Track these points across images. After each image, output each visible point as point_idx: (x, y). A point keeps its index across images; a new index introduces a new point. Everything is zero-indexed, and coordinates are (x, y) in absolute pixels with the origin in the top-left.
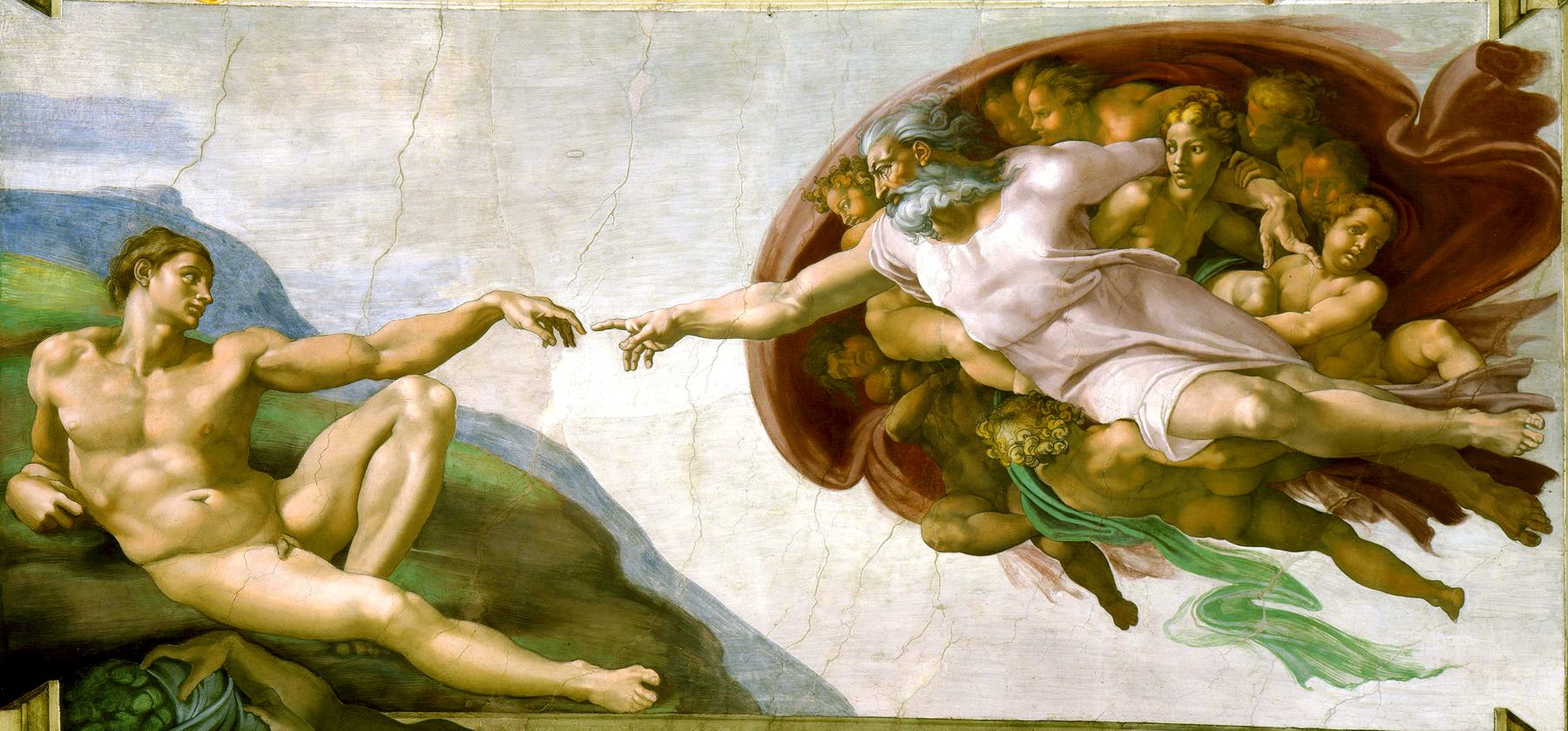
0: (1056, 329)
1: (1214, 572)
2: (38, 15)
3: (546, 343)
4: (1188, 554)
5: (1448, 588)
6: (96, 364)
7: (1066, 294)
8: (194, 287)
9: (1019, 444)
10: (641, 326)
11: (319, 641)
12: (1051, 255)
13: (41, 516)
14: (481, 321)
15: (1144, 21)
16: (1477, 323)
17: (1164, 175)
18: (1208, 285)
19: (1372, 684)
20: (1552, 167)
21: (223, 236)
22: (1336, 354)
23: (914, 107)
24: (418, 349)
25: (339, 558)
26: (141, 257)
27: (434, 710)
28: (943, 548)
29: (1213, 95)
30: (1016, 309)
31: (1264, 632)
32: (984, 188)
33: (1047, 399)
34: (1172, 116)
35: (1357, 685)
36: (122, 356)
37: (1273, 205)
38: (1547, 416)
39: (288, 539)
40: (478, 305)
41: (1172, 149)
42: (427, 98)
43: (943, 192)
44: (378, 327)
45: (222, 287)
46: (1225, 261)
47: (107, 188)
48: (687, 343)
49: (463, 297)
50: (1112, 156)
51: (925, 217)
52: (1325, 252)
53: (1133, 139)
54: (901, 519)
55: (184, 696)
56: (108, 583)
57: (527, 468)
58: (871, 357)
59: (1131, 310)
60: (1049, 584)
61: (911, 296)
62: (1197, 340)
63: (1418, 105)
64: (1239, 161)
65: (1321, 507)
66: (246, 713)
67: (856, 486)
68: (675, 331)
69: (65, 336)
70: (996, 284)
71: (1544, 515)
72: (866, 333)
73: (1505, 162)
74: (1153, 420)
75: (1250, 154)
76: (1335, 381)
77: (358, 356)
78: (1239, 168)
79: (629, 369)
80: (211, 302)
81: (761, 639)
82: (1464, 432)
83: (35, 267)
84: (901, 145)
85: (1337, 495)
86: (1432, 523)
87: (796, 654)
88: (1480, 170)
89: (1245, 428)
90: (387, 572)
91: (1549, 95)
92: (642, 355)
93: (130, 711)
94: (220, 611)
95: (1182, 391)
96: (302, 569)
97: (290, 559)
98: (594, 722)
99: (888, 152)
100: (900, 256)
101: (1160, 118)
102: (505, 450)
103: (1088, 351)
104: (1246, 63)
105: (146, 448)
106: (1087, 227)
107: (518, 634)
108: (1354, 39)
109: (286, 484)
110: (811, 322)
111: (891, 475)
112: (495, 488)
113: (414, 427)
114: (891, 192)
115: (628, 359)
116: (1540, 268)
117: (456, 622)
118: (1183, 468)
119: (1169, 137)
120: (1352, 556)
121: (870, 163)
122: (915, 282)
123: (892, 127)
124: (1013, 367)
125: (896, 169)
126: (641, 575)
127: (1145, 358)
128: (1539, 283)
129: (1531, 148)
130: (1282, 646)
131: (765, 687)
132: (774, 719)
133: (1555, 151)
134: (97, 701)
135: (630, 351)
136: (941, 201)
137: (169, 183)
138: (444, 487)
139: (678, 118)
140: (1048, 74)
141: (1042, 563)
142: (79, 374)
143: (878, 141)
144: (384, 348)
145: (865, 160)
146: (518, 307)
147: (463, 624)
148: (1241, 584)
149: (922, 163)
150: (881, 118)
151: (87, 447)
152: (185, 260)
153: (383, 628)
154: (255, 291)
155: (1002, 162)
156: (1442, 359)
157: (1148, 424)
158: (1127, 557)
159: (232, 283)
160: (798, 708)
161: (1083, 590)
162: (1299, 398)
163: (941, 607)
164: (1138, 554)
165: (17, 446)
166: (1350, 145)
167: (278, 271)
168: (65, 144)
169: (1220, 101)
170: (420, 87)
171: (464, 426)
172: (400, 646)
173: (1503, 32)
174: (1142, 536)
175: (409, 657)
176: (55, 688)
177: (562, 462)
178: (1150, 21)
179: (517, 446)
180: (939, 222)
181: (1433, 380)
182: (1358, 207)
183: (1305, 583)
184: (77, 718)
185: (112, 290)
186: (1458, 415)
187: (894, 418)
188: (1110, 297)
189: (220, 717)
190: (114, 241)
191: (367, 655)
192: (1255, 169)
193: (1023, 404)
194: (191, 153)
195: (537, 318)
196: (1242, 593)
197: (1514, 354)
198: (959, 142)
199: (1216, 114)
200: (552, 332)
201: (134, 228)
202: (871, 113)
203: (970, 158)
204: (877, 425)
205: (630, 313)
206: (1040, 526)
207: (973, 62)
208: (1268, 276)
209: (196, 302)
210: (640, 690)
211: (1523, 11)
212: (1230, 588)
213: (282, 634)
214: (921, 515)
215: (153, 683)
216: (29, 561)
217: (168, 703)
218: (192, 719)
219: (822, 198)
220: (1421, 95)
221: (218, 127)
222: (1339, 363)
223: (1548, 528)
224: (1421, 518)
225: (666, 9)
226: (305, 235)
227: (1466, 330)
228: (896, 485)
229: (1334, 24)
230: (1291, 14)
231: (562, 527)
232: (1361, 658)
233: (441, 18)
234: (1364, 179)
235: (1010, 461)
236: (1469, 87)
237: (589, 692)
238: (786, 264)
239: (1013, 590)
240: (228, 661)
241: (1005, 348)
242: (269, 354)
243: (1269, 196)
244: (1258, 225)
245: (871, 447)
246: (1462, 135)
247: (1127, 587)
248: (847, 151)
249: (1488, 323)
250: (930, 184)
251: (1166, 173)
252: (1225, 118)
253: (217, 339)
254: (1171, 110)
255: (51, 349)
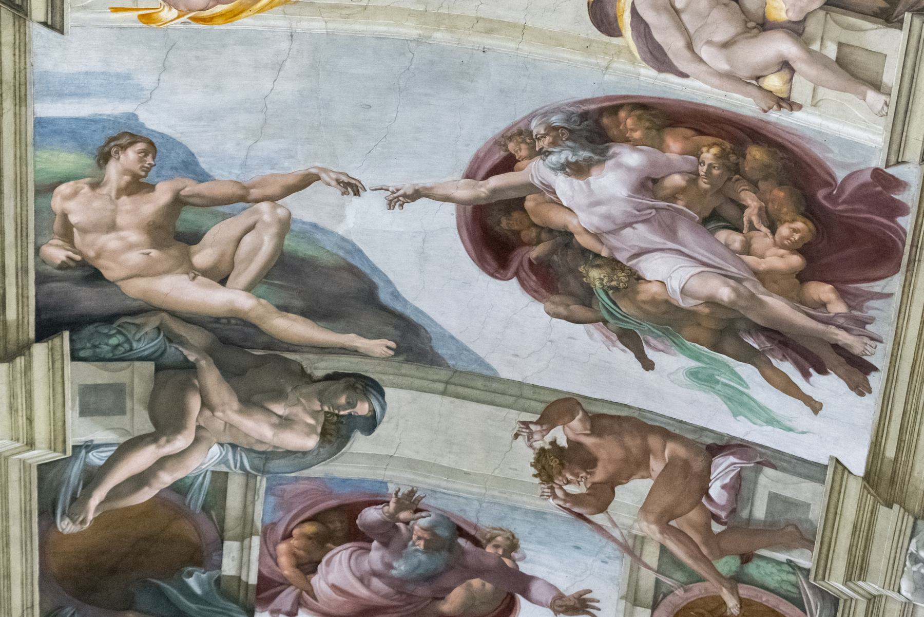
0: (628, 231)
1: (697, 359)
2: (58, 35)
3: (343, 194)
4: (684, 348)
5: (814, 400)
6: (89, 194)
7: (635, 216)
8: (145, 159)
9: (601, 279)
10: (398, 190)
11: (211, 317)
12: (629, 196)
13: (59, 262)
14: (307, 181)
15: (695, 101)
16: (849, 293)
17: (696, 175)
18: (712, 232)
19: (770, 428)
20: (901, 237)
21: (162, 135)
22: (775, 282)
23: (562, 112)
24: (269, 191)
25: (223, 282)
26: (115, 146)
27: (272, 350)
28: (555, 316)
29: (728, 145)
30: (608, 217)
31: (719, 390)
32: (596, 157)
33: (619, 262)
34: (704, 149)
35: (762, 426)
36: (104, 190)
37: (752, 205)
38: (878, 344)
39: (194, 272)
40: (306, 172)
41: (702, 164)
42: (281, 73)
43: (574, 155)
44: (248, 178)
45: (160, 159)
46: (724, 224)
47: (96, 114)
48: (423, 201)
49: (298, 167)
50: (668, 159)
51: (563, 164)
52: (776, 235)
53: (683, 153)
54: (534, 299)
55: (137, 337)
56: (96, 290)
57: (329, 249)
58: (527, 223)
59: (670, 232)
60: (609, 342)
61: (551, 198)
62: (703, 255)
63: (836, 185)
64: (737, 180)
65: (756, 346)
66: (170, 347)
67: (511, 280)
68: (416, 195)
69: (71, 183)
70: (598, 203)
71: (869, 385)
72: (524, 210)
73: (879, 227)
74: (675, 285)
75: (744, 178)
76: (774, 295)
77: (238, 191)
78: (737, 183)
79: (390, 209)
80: (155, 165)
81: (452, 337)
82: (835, 337)
83: (56, 153)
84: (550, 129)
85: (765, 344)
86: (811, 370)
87: (471, 347)
88: (862, 225)
89: (722, 300)
90: (249, 288)
91: (906, 203)
92: (398, 204)
93: (107, 344)
94: (157, 302)
95: (692, 276)
96: (201, 285)
97: (196, 281)
98: (360, 359)
99: (545, 130)
100: (546, 178)
101: (698, 148)
102: (318, 239)
103: (644, 245)
104: (748, 135)
105: (117, 231)
106: (651, 188)
107: (320, 321)
108: (807, 143)
109: (194, 248)
110: (493, 201)
111: (531, 279)
112: (311, 256)
113: (268, 225)
114: (544, 149)
115: (390, 204)
116: (886, 280)
117: (286, 313)
118: (685, 310)
119: (701, 158)
120: (769, 372)
121: (534, 134)
122: (554, 193)
123: (548, 119)
124: (602, 243)
125: (548, 139)
126: (389, 300)
127: (674, 256)
128: (885, 286)
129: (892, 224)
130: (728, 399)
131: (452, 357)
132: (456, 371)
133: (904, 230)
134: (89, 340)
135: (391, 201)
136: (572, 159)
137: (131, 111)
138: (282, 254)
139: (426, 95)
140: (638, 112)
141: (607, 334)
142: (80, 198)
143: (540, 124)
144: (253, 187)
145: (532, 132)
146: (329, 176)
147: (290, 315)
148: (710, 368)
149: (564, 139)
150: (542, 114)
151: (84, 231)
152: (140, 146)
153: (246, 313)
154: (180, 160)
155: (608, 148)
156: (829, 302)
157: (672, 288)
158: (653, 341)
159: (167, 156)
160: (469, 369)
161: (627, 349)
162: (753, 296)
163: (551, 341)
164: (658, 341)
165: (45, 232)
166: (798, 192)
167: (193, 150)
168: (72, 95)
169: (731, 149)
170: (279, 67)
171: (292, 227)
172: (256, 322)
173: (887, 166)
174: (661, 334)
175: (259, 327)
176: (66, 334)
177: (349, 247)
178: (698, 102)
179: (324, 238)
180: (570, 168)
181: (823, 310)
182: (798, 221)
183: (743, 376)
184: (78, 346)
185: (98, 161)
186: (832, 329)
187: (535, 253)
188: (659, 222)
189: (156, 347)
190: (99, 139)
191: (237, 324)
192: (745, 186)
193: (605, 261)
194: (144, 96)
195: (339, 182)
196: (710, 371)
197: (866, 313)
198: (585, 134)
199: (728, 154)
200: (347, 189)
201: (111, 133)
202: (538, 110)
203: (591, 142)
204: (525, 254)
205: (392, 185)
206: (607, 317)
207: (597, 98)
208: (745, 237)
209: (146, 165)
210: (386, 349)
211: (900, 160)
212: (703, 368)
213: (191, 313)
214: (545, 300)
215: (120, 332)
216: (53, 281)
217: (128, 340)
218: (141, 348)
219: (505, 145)
220: (839, 181)
221: (161, 84)
222: (776, 287)
223: (870, 392)
224: (807, 367)
225: (423, 41)
226: (210, 134)
227: (843, 295)
228: (532, 284)
229: (798, 133)
230: (775, 121)
231: (345, 275)
232: (766, 415)
233: (292, 36)
234: (802, 209)
235: (595, 286)
236: (864, 185)
237: (357, 347)
238: (482, 173)
239: (590, 341)
240: (161, 324)
241: (600, 234)
242: (187, 189)
243: (751, 201)
244: (744, 212)
245: (521, 264)
246: (856, 207)
247: (650, 353)
248: (522, 126)
249: (856, 296)
250: (566, 150)
251: (698, 175)
252: (733, 158)
253: (158, 182)
254: (704, 146)
255: (64, 189)
